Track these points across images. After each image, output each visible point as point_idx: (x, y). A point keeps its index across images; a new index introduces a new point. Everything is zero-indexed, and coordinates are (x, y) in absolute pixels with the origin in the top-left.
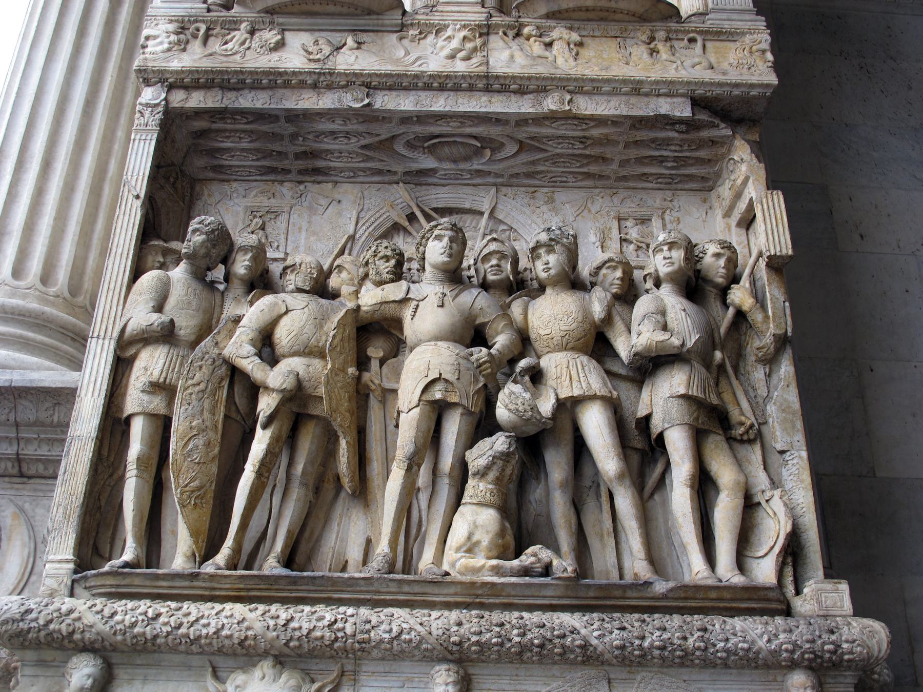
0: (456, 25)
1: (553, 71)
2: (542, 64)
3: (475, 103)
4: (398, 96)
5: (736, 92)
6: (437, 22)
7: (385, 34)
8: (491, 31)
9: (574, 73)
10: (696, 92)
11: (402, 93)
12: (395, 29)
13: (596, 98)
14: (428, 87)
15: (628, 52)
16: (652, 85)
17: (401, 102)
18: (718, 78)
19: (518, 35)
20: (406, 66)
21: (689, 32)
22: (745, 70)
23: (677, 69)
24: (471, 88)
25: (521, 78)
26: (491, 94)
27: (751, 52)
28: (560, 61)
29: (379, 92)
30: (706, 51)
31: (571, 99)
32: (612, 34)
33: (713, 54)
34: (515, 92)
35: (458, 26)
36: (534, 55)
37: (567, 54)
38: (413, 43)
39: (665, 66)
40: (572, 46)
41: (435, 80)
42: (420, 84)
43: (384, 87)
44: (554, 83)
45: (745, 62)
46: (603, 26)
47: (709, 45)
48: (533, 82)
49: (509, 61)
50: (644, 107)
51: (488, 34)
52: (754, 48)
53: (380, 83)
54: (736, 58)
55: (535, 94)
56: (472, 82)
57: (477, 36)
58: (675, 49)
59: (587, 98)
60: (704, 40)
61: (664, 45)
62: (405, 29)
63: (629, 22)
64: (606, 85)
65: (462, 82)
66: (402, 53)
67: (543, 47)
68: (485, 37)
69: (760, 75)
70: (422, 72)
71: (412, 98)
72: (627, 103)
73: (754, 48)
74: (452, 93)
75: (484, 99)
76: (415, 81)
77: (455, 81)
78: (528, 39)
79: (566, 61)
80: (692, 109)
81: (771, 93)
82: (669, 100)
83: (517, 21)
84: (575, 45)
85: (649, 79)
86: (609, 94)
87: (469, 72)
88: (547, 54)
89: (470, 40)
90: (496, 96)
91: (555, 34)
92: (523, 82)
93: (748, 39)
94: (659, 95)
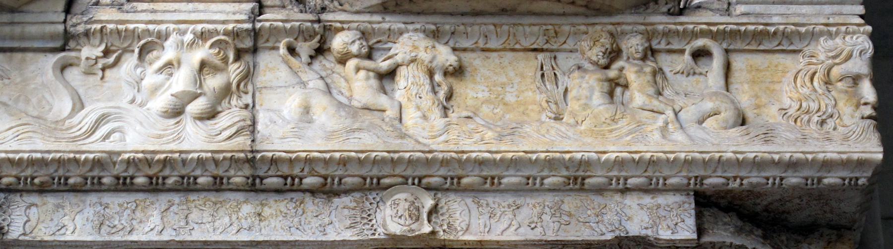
0: (184, 33)
1: (395, 144)
2: (372, 126)
3: (226, 220)
4: (58, 207)
5: (793, 179)
6: (142, 26)
7: (30, 55)
8: (261, 43)
9: (442, 147)
10: (706, 182)
11: (72, 198)
12: (51, 45)
13: (490, 200)
14: (124, 185)
15: (561, 89)
16: (610, 170)
17: (66, 220)
18: (754, 149)
19: (321, 50)
20: (74, 140)
21: (695, 35)
22: (813, 126)
23: (664, 130)
24: (219, 185)
25: (326, 162)
26: (262, 196)
27: (828, 82)
28: (411, 117)
29: (17, 198)
30: (732, 80)
31: (436, 206)
32: (526, 44)
33: (746, 86)
34: (313, 192)
35: (189, 37)
36: (355, 103)
37: (427, 100)
38: (91, 79)
39: (640, 124)
40: (438, 78)
41: (139, 170)
42: (105, 180)
43: (29, 187)
44: (398, 171)
45: (814, 106)
46: (505, 28)
47: (739, 62)
48: (353, 170)
49: (301, 121)
50: (593, 219)
51: (255, 50)
52: (836, 72)
53: (19, 179)
54: (795, 96)
55: (357, 195)
56: (220, 172)
57: (231, 56)
58: (665, 78)
59: (469, 201)
60: (727, 51)
61: (640, 71)
62: (72, 44)
63: (564, 14)
64: (511, 172)
65: (198, 172)
66: (65, 105)
67: (374, 82)
68: (248, 58)
69: (846, 138)
70: (110, 153)
71: (89, 212)
72: (557, 210)
73: (836, 72)
74: (176, 198)
75: (247, 209)
76: (96, 173)
77: (184, 172)
78: (343, 60)
79: (425, 117)
80: (699, 216)
81: (869, 179)
82: (647, 200)
83: (319, 21)
84: (446, 74)
85: (604, 157)
86: (516, 190)
87: (213, 152)
88: (382, 100)
89: (216, 69)
90: (271, 201)
91: (401, 50)
92: (330, 171)
93: (822, 48)
94: (625, 191)
